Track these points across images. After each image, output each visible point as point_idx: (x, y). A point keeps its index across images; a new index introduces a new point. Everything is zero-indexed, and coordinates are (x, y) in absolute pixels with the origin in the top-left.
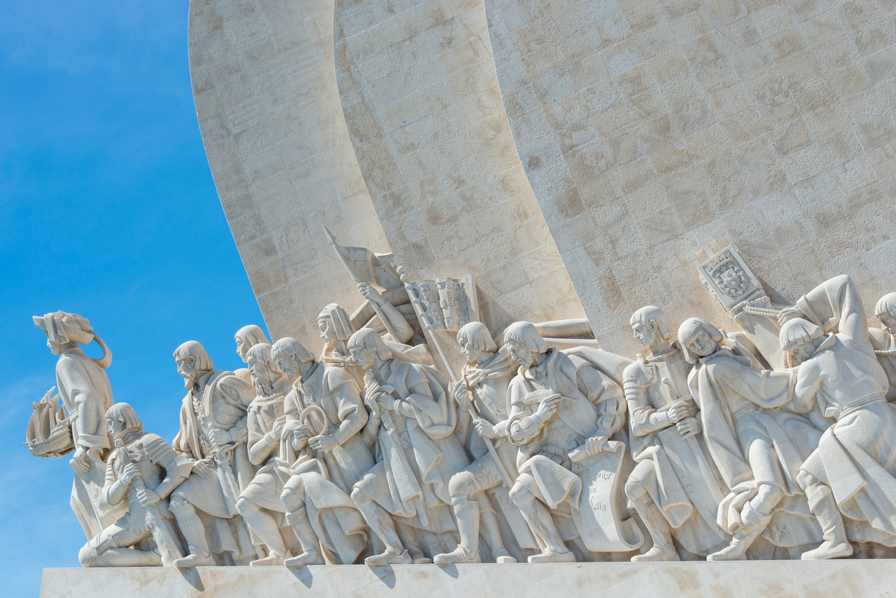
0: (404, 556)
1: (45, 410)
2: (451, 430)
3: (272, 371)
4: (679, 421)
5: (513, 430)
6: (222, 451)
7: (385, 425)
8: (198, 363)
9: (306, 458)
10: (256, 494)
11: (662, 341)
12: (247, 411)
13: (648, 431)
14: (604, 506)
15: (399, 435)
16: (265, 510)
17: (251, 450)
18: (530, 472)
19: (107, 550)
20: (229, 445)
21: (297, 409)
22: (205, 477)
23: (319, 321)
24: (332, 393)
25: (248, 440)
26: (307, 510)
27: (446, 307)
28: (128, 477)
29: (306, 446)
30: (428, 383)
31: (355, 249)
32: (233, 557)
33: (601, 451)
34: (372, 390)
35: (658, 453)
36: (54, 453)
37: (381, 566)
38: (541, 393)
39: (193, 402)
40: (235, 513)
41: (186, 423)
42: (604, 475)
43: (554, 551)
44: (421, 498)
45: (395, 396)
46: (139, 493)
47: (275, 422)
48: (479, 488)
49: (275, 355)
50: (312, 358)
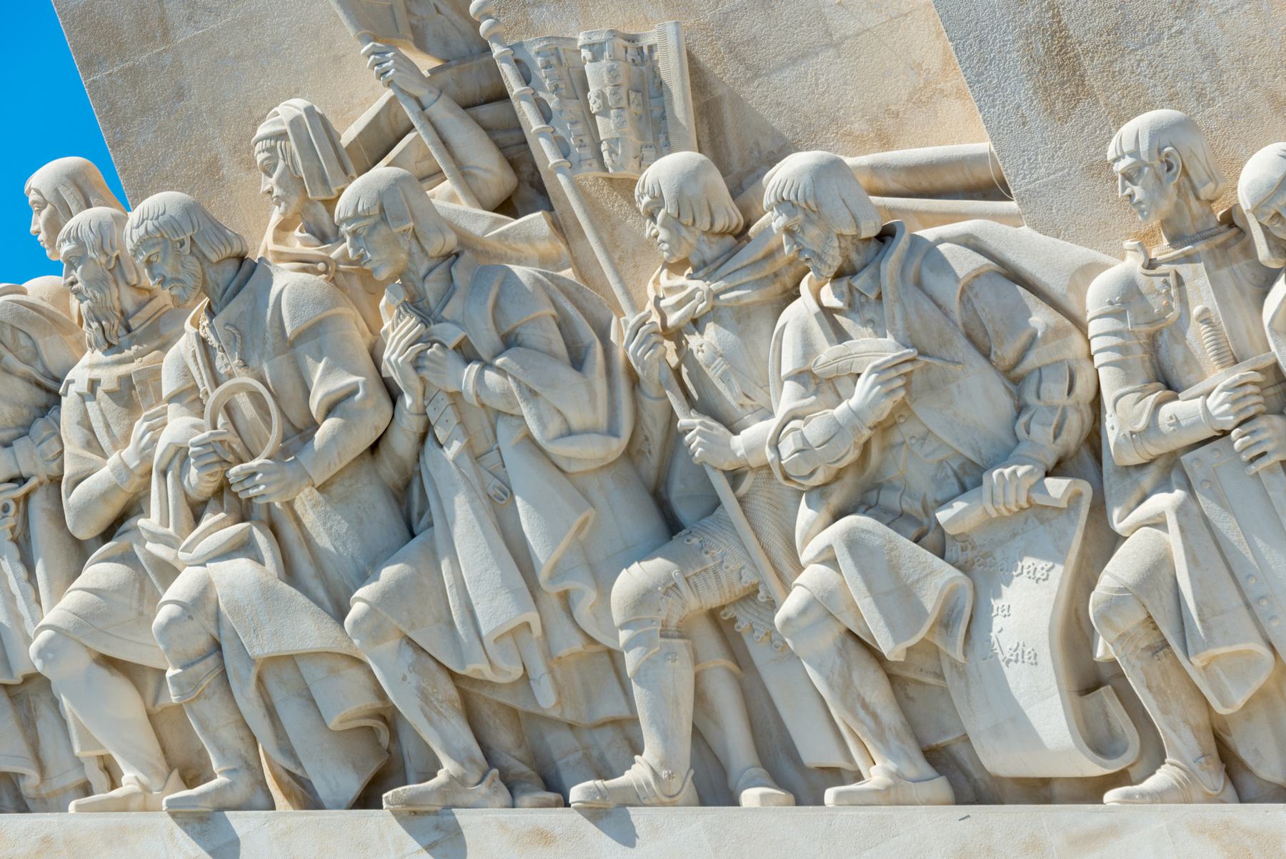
0: (490, 786)
2: (617, 445)
3: (128, 283)
4: (1239, 425)
5: (788, 446)
7: (440, 433)
9: (223, 519)
10: (86, 619)
11: (1194, 204)
12: (61, 391)
13: (1154, 451)
14: (1032, 654)
15: (477, 459)
16: (109, 662)
17: (72, 500)
18: (832, 562)
21: (196, 388)
23: (259, 147)
25: (63, 471)
26: (226, 661)
27: (605, 112)
29: (223, 489)
30: (554, 317)
32: (23, 793)
33: (1025, 505)
35: (1181, 511)
37: (427, 813)
38: (863, 348)
40: (29, 671)
42: (1032, 569)
43: (897, 776)
45: (466, 353)
47: (137, 423)
48: (693, 603)
49: (135, 241)
50: (237, 249)
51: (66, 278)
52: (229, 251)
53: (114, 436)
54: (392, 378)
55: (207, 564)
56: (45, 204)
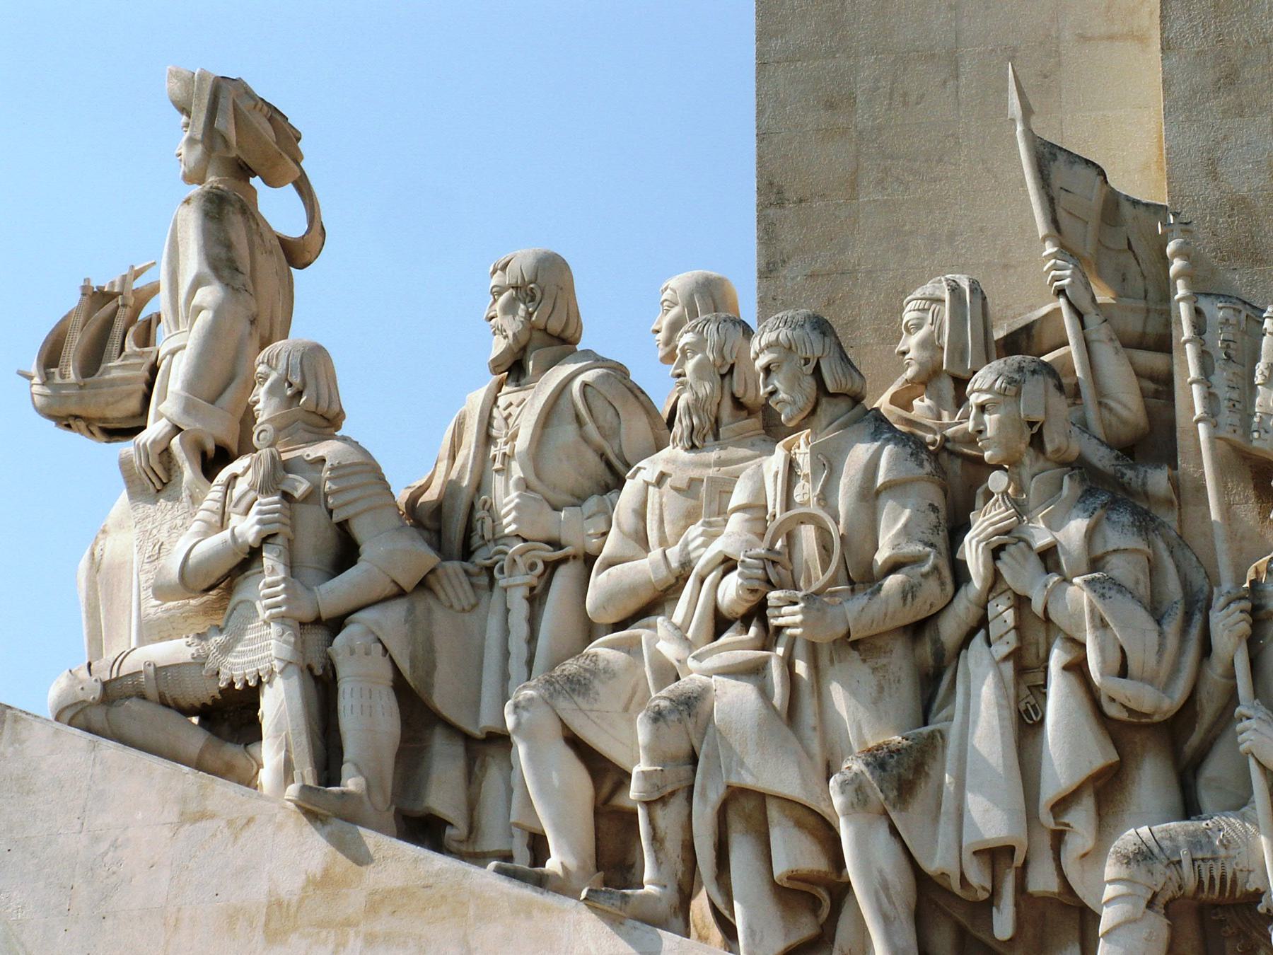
1: (109, 307)
6: (523, 553)
7: (995, 629)
8: (546, 306)
15: (1021, 671)
16: (575, 743)
17: (600, 581)
19: (128, 697)
20: (547, 547)
21: (766, 507)
22: (451, 606)
24: (878, 493)
28: (257, 527)
29: (757, 612)
31: (1074, 159)
34: (992, 524)
36: (89, 421)
39: (495, 410)
41: (453, 457)
44: (1019, 860)
46: (268, 579)
49: (763, 344)
51: (676, 368)
52: (849, 386)
53: (664, 532)
54: (965, 562)
55: (714, 676)
56: (676, 304)
